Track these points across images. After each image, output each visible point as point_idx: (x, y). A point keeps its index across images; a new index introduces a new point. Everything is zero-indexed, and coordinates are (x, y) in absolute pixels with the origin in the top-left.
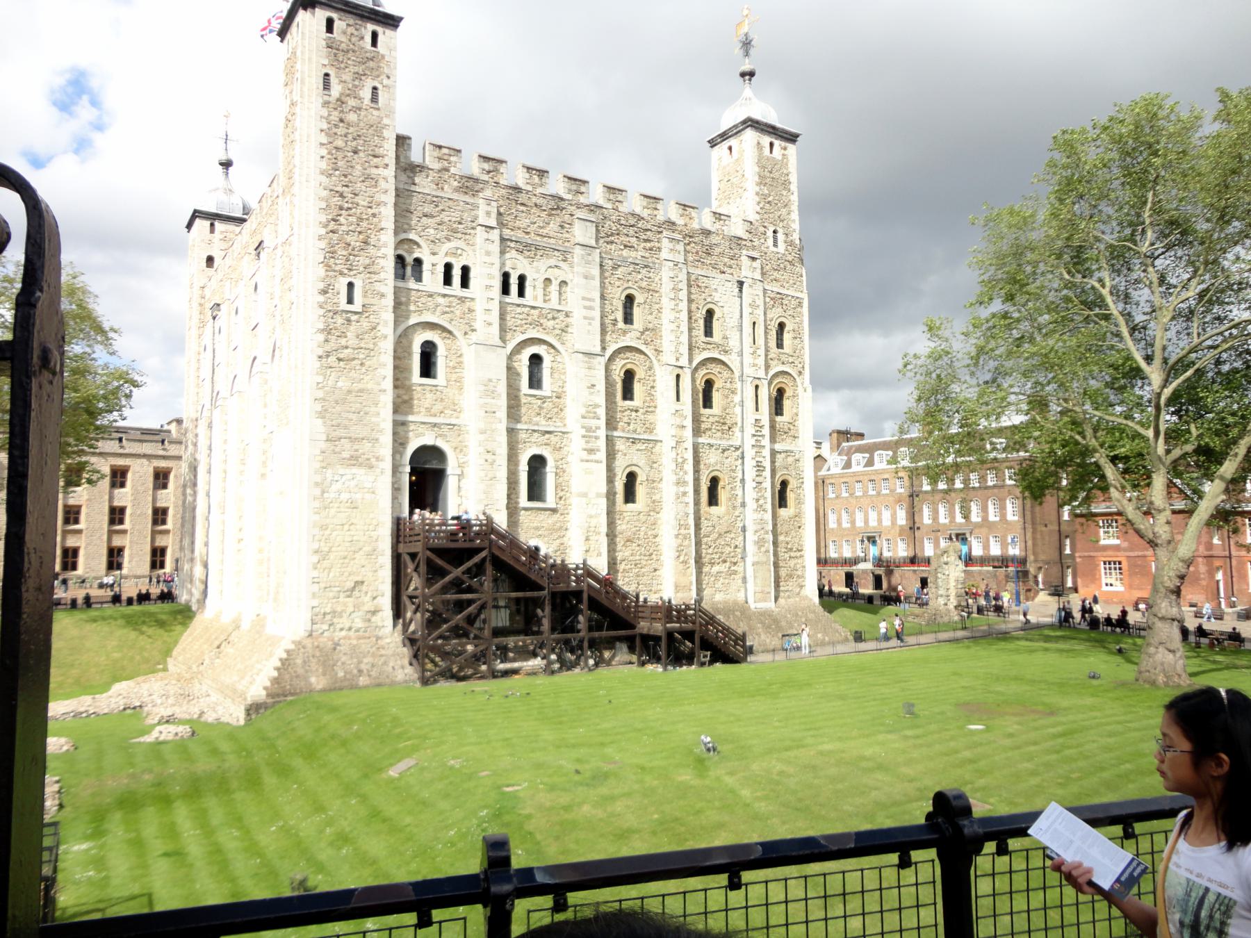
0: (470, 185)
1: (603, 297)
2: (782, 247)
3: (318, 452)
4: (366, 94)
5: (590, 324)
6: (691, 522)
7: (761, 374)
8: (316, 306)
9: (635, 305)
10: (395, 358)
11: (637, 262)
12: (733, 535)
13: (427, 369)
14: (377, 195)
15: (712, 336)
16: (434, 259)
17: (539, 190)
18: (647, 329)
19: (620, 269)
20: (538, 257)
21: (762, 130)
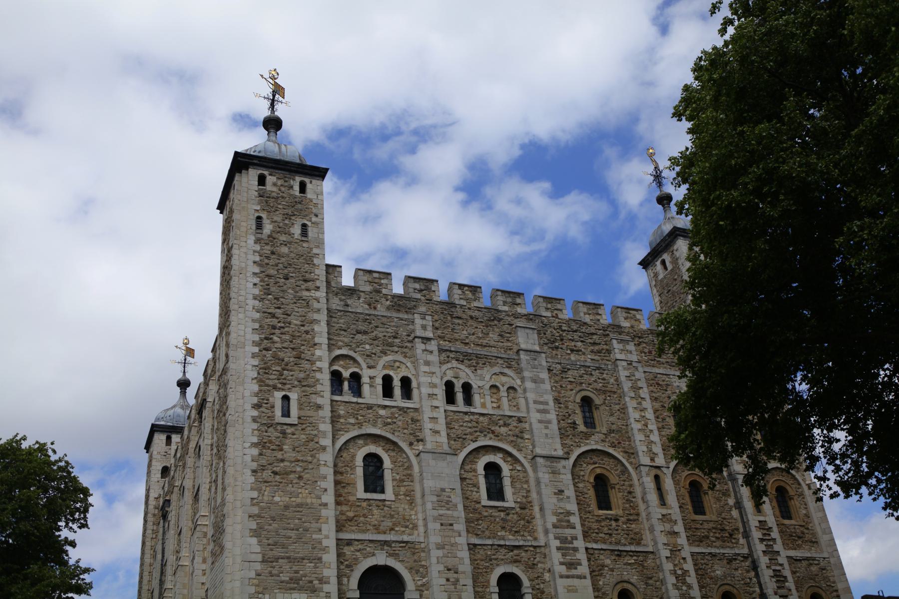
1: (557, 400)
3: (253, 574)
4: (297, 230)
5: (547, 428)
8: (249, 420)
9: (594, 408)
10: (336, 473)
11: (588, 364)
13: (374, 481)
14: (310, 315)
16: (371, 372)
17: (476, 304)
19: (570, 372)
20: (480, 365)
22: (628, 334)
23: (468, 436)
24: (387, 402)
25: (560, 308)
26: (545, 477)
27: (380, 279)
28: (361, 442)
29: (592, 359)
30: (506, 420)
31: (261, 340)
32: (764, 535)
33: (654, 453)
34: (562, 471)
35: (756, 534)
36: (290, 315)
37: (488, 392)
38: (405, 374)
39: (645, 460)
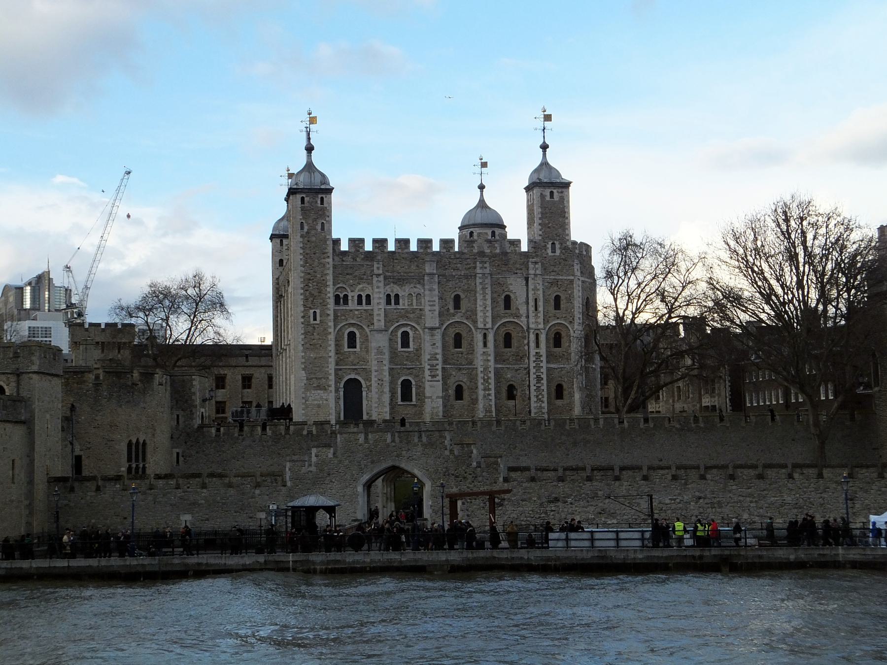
1: (441, 298)
2: (558, 252)
3: (303, 385)
4: (319, 227)
5: (432, 313)
6: (493, 409)
7: (541, 326)
8: (300, 323)
10: (336, 341)
12: (523, 415)
13: (352, 343)
15: (510, 309)
16: (352, 294)
17: (406, 251)
18: (467, 311)
19: (451, 282)
22: (487, 256)
24: (359, 308)
26: (427, 337)
28: (347, 327)
30: (413, 312)
31: (304, 286)
32: (537, 359)
35: (532, 359)
37: (406, 298)
39: (480, 325)
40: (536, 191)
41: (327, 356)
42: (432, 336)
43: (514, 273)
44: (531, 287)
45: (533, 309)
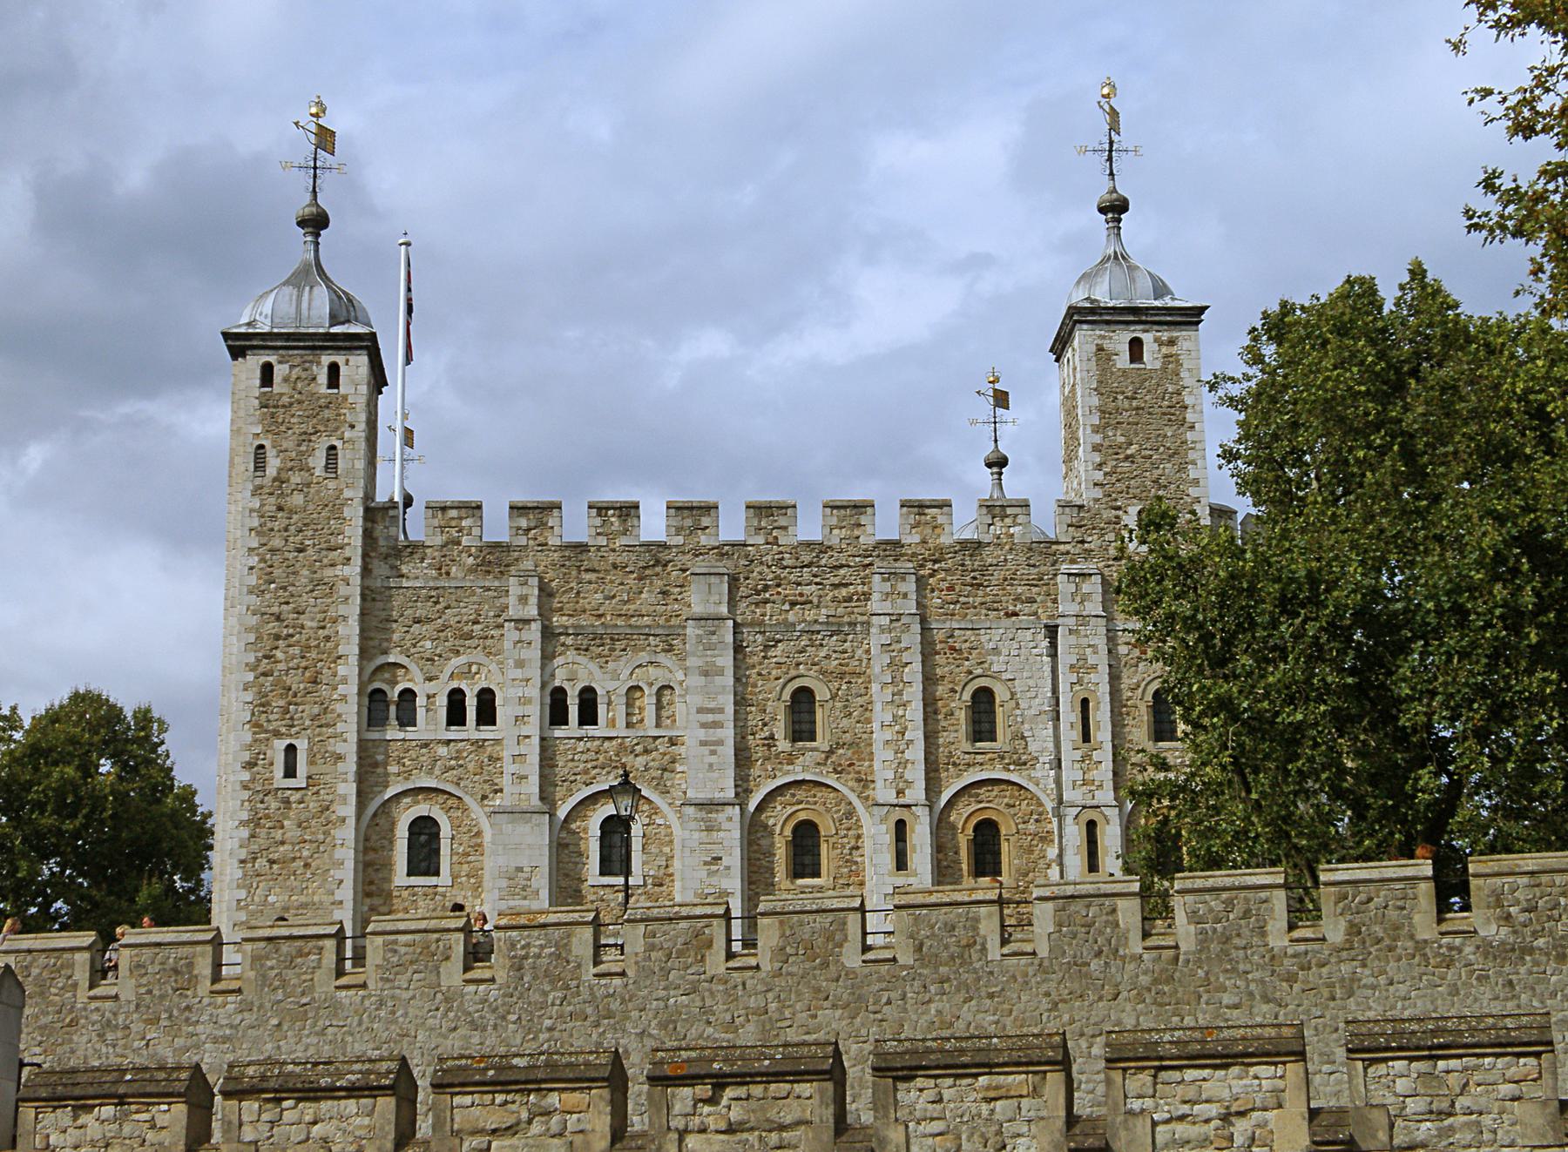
0: (495, 559)
4: (318, 461)
5: (713, 753)
8: (238, 787)
10: (366, 850)
11: (817, 627)
16: (431, 687)
17: (624, 540)
21: (1108, 323)
23: (578, 777)
24: (455, 733)
25: (785, 524)
27: (461, 518)
28: (408, 800)
29: (828, 616)
31: (258, 660)
33: (906, 781)
34: (725, 825)
36: (303, 613)
38: (485, 685)
40: (1083, 339)
41: (327, 899)
42: (709, 829)
43: (1008, 615)
44: (1065, 658)
45: (1076, 734)
